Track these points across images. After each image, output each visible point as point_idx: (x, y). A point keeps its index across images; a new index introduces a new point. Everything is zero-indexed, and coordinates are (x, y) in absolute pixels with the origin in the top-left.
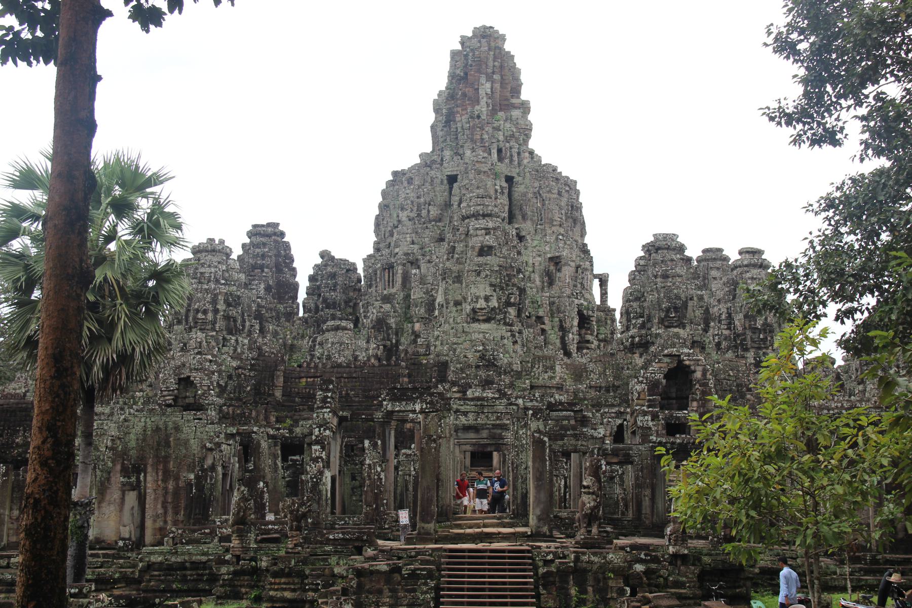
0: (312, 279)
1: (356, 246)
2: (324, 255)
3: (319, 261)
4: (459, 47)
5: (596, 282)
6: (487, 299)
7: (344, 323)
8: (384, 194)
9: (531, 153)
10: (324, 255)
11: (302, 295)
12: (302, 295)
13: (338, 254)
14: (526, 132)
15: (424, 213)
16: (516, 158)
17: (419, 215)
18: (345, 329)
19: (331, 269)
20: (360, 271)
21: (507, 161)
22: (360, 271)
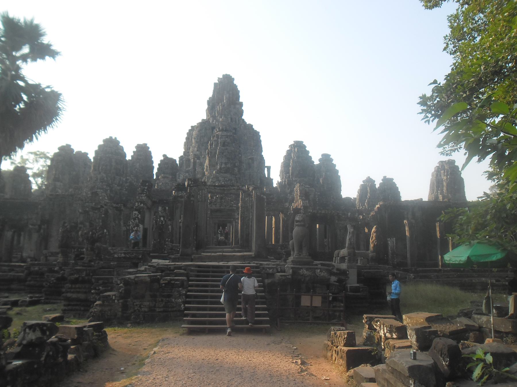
0: (159, 165)
1: (176, 153)
2: (165, 156)
3: (162, 158)
4: (217, 82)
5: (266, 169)
6: (226, 164)
7: (167, 176)
8: (187, 133)
9: (243, 120)
10: (165, 156)
11: (155, 171)
12: (155, 171)
13: (169, 156)
14: (241, 113)
15: (202, 140)
16: (237, 122)
17: (200, 141)
18: (167, 178)
19: (167, 162)
20: (178, 162)
21: (234, 122)
22: (178, 162)
